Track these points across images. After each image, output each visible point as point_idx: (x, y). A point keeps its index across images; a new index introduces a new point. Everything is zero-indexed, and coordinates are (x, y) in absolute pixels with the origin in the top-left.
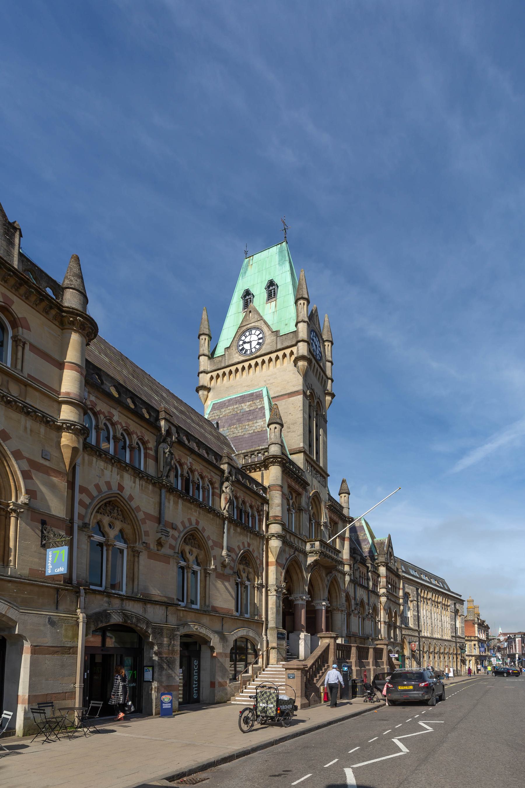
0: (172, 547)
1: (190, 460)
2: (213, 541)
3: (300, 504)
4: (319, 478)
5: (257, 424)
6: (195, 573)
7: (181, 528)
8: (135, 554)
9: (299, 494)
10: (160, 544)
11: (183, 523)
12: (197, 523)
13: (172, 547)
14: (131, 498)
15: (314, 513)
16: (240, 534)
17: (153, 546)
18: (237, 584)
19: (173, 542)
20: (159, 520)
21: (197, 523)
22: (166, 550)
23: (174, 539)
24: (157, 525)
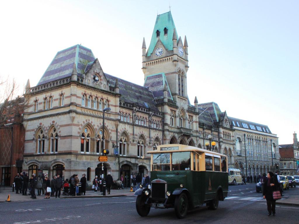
0: (136, 141)
1: (140, 114)
2: (147, 136)
3: (175, 115)
5: (160, 87)
6: (142, 146)
7: (138, 135)
8: (128, 145)
9: (175, 111)
10: (133, 141)
11: (139, 133)
12: (142, 132)
13: (136, 141)
14: (127, 130)
15: (182, 115)
16: (155, 132)
17: (132, 142)
19: (136, 139)
20: (133, 134)
21: (142, 132)
22: (135, 142)
23: (137, 139)
24: (132, 136)
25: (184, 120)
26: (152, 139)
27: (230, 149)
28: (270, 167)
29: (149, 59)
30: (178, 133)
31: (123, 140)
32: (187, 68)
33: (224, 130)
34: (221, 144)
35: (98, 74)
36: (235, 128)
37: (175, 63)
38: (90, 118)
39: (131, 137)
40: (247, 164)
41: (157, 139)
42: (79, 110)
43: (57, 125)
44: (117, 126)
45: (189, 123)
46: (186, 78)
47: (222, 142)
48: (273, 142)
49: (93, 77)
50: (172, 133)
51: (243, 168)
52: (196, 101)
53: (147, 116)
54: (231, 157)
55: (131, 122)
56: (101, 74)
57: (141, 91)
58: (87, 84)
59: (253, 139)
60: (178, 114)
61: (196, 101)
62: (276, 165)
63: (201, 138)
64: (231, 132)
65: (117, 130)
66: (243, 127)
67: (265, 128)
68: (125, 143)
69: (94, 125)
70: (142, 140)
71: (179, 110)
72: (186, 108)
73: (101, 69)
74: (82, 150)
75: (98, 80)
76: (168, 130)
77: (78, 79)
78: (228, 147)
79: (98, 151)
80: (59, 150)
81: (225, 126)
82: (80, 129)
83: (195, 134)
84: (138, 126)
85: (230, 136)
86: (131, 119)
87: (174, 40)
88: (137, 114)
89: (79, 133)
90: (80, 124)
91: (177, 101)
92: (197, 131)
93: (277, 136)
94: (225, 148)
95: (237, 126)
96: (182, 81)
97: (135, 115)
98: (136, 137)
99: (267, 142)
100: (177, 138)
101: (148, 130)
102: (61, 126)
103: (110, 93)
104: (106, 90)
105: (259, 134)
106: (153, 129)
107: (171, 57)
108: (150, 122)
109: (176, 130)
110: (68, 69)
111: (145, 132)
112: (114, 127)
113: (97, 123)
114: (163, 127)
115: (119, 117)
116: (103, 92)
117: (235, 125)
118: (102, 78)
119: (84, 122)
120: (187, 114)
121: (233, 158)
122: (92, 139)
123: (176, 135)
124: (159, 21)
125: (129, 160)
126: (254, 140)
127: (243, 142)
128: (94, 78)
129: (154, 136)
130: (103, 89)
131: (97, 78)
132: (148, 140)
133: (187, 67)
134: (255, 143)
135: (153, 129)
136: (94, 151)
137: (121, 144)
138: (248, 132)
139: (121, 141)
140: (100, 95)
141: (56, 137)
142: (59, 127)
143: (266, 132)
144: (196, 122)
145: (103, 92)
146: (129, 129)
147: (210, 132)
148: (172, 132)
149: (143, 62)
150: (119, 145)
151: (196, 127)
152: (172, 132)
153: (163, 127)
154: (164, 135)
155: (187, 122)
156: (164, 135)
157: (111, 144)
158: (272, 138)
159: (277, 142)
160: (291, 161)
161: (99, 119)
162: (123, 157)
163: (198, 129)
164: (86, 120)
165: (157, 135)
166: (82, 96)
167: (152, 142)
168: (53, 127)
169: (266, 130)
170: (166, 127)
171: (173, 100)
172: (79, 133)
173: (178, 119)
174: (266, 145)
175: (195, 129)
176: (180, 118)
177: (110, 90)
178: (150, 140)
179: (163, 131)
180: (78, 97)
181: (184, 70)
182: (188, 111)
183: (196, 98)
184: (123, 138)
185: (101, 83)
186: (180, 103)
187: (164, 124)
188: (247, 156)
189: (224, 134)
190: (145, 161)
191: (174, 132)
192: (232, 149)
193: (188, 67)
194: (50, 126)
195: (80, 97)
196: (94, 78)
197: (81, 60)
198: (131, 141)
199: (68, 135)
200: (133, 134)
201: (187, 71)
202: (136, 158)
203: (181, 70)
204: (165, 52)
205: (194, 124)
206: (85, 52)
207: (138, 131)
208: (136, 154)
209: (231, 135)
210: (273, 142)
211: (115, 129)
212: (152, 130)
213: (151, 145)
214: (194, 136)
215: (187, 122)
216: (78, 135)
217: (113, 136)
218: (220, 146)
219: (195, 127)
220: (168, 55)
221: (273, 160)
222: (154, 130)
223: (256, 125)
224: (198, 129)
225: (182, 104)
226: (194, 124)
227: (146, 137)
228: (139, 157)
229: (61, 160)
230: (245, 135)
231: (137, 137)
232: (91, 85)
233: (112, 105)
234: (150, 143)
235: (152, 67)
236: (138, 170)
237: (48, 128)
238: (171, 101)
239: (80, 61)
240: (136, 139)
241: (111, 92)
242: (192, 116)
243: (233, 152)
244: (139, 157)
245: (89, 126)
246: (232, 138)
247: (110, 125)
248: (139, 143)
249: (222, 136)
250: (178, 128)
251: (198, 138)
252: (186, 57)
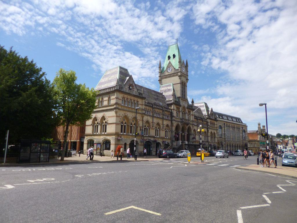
4: (185, 102)
6: (158, 130)
9: (179, 108)
10: (153, 127)
13: (155, 127)
17: (152, 128)
18: (165, 131)
19: (154, 126)
20: (153, 122)
22: (154, 128)
23: (155, 125)
25: (185, 114)
26: (164, 126)
27: (214, 133)
28: (241, 146)
30: (181, 122)
31: (147, 126)
32: (187, 81)
33: (211, 120)
34: (209, 129)
35: (132, 85)
36: (218, 119)
38: (127, 112)
39: (151, 124)
40: (226, 143)
41: (167, 126)
42: (120, 107)
43: (106, 116)
44: (143, 117)
45: (188, 116)
47: (209, 128)
48: (244, 129)
49: (128, 87)
51: (223, 146)
53: (161, 111)
54: (215, 138)
55: (152, 115)
56: (134, 85)
57: (158, 95)
58: (125, 91)
59: (230, 127)
60: (181, 110)
61: (193, 102)
62: (245, 144)
63: (196, 125)
64: (215, 122)
65: (143, 119)
66: (224, 119)
67: (238, 120)
68: (148, 128)
69: (129, 117)
70: (158, 126)
72: (186, 106)
73: (134, 82)
74: (122, 132)
75: (132, 89)
76: (175, 120)
77: (120, 88)
78: (213, 131)
79: (131, 133)
80: (107, 131)
81: (211, 118)
82: (120, 119)
83: (191, 123)
84: (155, 117)
85: (215, 125)
86: (152, 113)
88: (155, 110)
89: (120, 121)
90: (121, 116)
91: (181, 101)
92: (193, 121)
93: (247, 125)
94: (211, 132)
95: (220, 118)
96: (184, 89)
97: (154, 111)
98: (154, 124)
99: (239, 129)
100: (180, 125)
101: (162, 120)
102: (109, 117)
103: (139, 96)
104: (136, 95)
105: (234, 124)
106: (165, 119)
108: (163, 115)
109: (180, 120)
110: (113, 82)
111: (160, 122)
112: (141, 117)
113: (131, 115)
114: (172, 118)
115: (144, 112)
116: (135, 96)
117: (218, 117)
118: (134, 87)
119: (123, 115)
120: (187, 110)
121: (216, 139)
122: (127, 125)
125: (150, 138)
126: (231, 127)
127: (223, 129)
128: (129, 88)
130: (134, 94)
131: (131, 88)
132: (162, 126)
133: (187, 80)
134: (231, 129)
135: (165, 119)
136: (128, 133)
137: (145, 129)
138: (227, 122)
139: (145, 126)
140: (132, 98)
141: (106, 123)
142: (107, 117)
143: (239, 122)
144: (193, 115)
145: (135, 96)
146: (150, 119)
147: (201, 121)
150: (144, 129)
151: (193, 118)
153: (172, 118)
154: (172, 123)
155: (187, 115)
156: (172, 123)
157: (139, 128)
158: (243, 126)
159: (247, 129)
160: (256, 142)
161: (132, 113)
162: (146, 136)
163: (194, 120)
164: (124, 114)
166: (122, 99)
167: (164, 127)
168: (103, 118)
169: (239, 121)
170: (174, 118)
172: (120, 121)
173: (181, 113)
174: (239, 131)
175: (192, 119)
176: (182, 113)
177: (139, 95)
178: (163, 126)
179: (172, 121)
180: (119, 99)
181: (186, 81)
182: (187, 108)
184: (147, 125)
185: (134, 91)
186: (182, 103)
187: (172, 116)
188: (226, 138)
189: (210, 123)
190: (160, 139)
191: (178, 122)
192: (216, 132)
194: (102, 116)
195: (121, 99)
196: (129, 88)
197: (121, 76)
198: (151, 126)
199: (113, 122)
200: (153, 122)
201: (187, 82)
202: (154, 137)
204: (173, 70)
205: (191, 116)
206: (123, 71)
207: (156, 120)
208: (154, 135)
209: (215, 124)
210: (244, 129)
211: (142, 119)
213: (164, 129)
214: (191, 124)
215: (187, 115)
216: (119, 123)
217: (140, 123)
218: (208, 131)
219: (192, 118)
221: (244, 141)
223: (232, 117)
224: (194, 120)
225: (184, 103)
226: (191, 116)
227: (160, 124)
228: (156, 136)
229: (108, 138)
230: (224, 124)
231: (155, 124)
232: (127, 91)
233: (140, 104)
234: (163, 128)
236: (155, 145)
237: (101, 118)
238: (177, 102)
239: (121, 77)
240: (154, 126)
241: (140, 96)
242: (190, 112)
243: (216, 135)
244: (156, 136)
245: (126, 117)
246: (216, 126)
247: (139, 117)
248: (156, 128)
249: (209, 124)
250: (181, 119)
251: (193, 126)
252: (187, 73)
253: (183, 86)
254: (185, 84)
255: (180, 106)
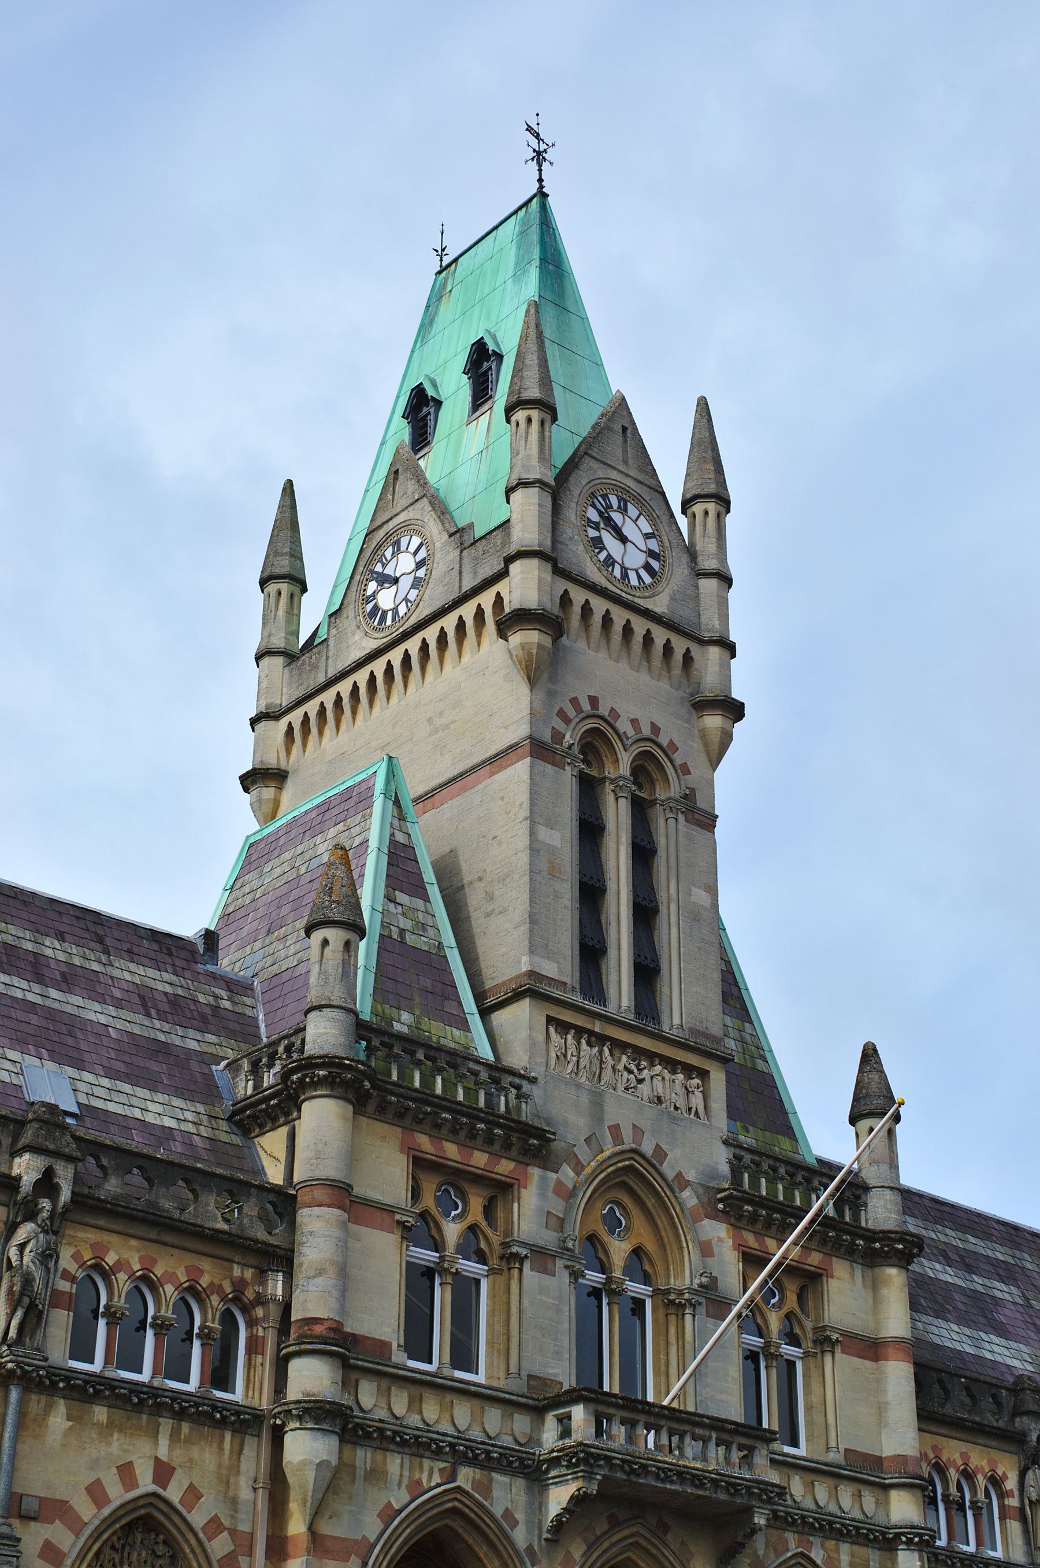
9: (500, 1191)
15: (638, 1252)
16: (111, 1426)
29: (310, 685)
32: (713, 721)
37: (516, 639)
46: (708, 821)
50: (431, 1475)
52: (873, 1101)
61: (873, 1101)
71: (567, 1173)
87: (520, 415)
107: (487, 599)
120: (717, 1231)
123: (506, 1494)
124: (447, 310)
129: (96, 1492)
148: (419, 1445)
149: (254, 722)
152: (419, 1445)
165: (163, 1472)
171: (485, 1052)
183: (870, 1056)
191: (461, 1452)
193: (736, 710)
203: (624, 726)
204: (445, 556)
212: (61, 1407)
219: (873, 1410)
220: (468, 585)
222: (100, 1413)
235: (330, 743)
253: (617, 815)
254: (647, 767)
255: (534, 1143)
